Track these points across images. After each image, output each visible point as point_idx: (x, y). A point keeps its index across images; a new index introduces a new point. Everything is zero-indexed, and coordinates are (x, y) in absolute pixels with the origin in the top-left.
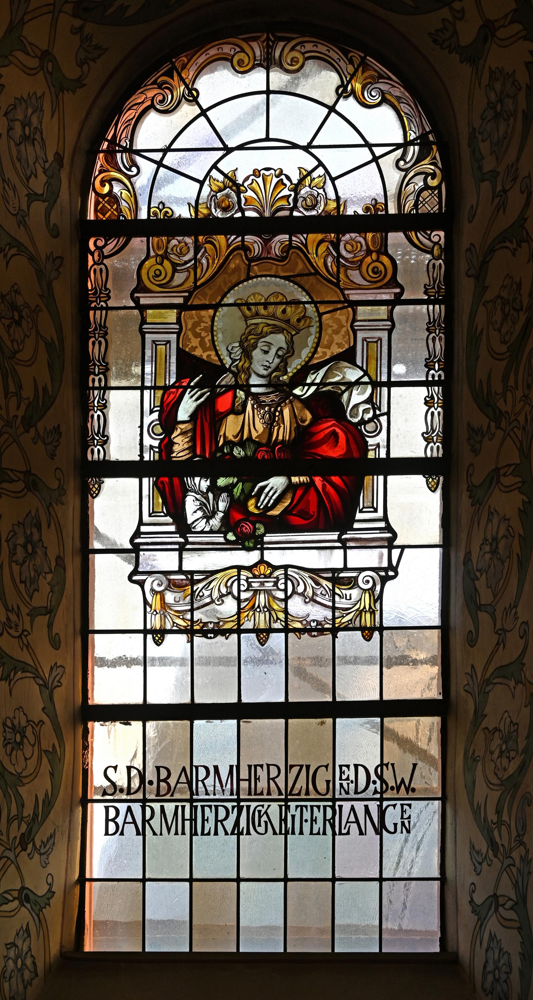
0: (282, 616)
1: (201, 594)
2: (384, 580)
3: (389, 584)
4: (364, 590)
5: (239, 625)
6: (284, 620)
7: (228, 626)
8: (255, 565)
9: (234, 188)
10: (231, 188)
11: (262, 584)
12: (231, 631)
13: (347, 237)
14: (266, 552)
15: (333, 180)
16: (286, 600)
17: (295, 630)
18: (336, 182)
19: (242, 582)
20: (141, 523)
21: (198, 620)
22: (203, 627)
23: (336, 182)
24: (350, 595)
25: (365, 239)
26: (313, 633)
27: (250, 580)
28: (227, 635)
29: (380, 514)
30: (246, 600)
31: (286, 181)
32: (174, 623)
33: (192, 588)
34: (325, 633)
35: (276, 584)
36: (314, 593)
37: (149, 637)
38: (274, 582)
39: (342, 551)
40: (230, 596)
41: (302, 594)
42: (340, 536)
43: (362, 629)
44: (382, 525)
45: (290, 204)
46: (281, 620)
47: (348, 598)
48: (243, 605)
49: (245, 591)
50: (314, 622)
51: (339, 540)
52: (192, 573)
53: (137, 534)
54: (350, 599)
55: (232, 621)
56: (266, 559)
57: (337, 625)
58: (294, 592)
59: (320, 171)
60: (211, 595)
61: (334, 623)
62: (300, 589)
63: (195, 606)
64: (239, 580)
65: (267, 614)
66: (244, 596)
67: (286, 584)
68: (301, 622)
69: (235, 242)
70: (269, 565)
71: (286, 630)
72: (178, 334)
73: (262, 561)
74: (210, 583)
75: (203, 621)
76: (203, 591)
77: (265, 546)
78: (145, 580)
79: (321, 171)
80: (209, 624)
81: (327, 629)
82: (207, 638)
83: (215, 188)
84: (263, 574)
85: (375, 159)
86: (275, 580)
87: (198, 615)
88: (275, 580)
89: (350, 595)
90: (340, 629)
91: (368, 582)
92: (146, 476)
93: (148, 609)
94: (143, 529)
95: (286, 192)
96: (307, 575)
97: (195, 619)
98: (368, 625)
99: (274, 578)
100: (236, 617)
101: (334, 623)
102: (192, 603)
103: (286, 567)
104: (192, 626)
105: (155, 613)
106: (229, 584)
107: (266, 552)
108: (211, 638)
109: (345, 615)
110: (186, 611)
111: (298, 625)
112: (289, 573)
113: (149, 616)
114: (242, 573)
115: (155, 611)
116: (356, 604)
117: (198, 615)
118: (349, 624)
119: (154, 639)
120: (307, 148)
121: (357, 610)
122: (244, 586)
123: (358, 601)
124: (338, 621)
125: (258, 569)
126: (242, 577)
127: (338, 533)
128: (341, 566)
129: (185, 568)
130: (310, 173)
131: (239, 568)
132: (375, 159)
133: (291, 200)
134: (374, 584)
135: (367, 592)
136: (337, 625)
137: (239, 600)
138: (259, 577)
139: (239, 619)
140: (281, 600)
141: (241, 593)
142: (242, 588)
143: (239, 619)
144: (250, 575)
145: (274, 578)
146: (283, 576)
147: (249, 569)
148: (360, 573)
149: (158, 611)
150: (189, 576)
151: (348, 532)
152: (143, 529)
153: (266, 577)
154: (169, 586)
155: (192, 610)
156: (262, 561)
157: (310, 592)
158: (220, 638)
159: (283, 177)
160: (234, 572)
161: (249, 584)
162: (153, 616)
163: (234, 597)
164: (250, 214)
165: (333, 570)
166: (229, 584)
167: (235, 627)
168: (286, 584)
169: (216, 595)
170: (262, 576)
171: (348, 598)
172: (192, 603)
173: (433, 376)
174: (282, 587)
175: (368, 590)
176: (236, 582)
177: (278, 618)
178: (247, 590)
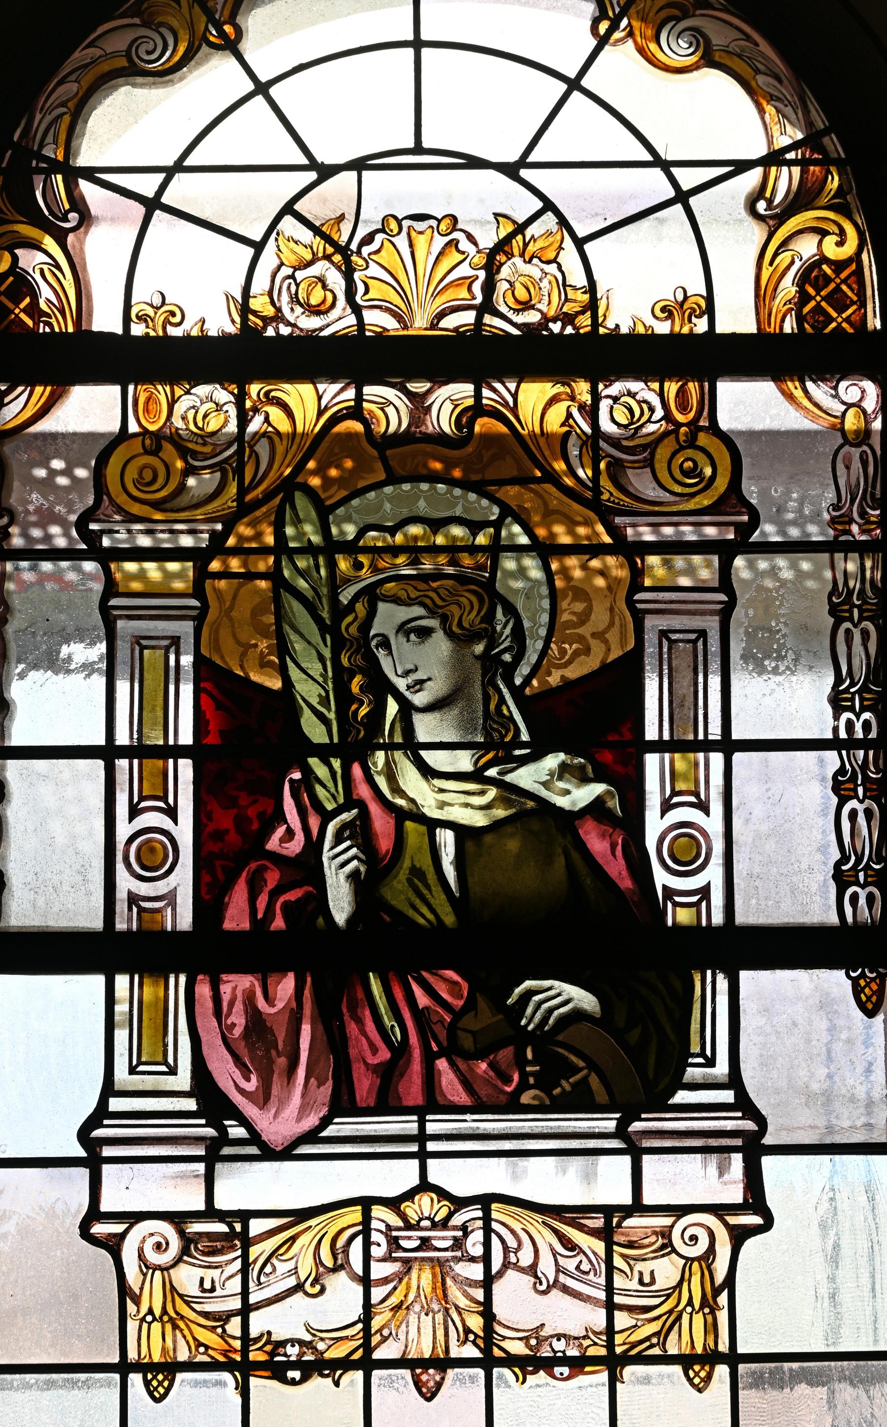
0: (476, 1323)
1: (268, 1269)
2: (739, 1236)
3: (751, 1245)
4: (689, 1260)
5: (367, 1347)
6: (481, 1334)
7: (338, 1352)
8: (409, 1195)
9: (337, 258)
10: (327, 257)
11: (425, 1244)
12: (345, 1364)
13: (616, 388)
14: (431, 1163)
15: (580, 243)
16: (488, 1282)
17: (510, 1361)
18: (588, 247)
19: (375, 1237)
20: (109, 1089)
21: (262, 1335)
22: (273, 1354)
23: (588, 247)
24: (652, 1272)
25: (661, 394)
26: (557, 1370)
27: (394, 1233)
28: (338, 1373)
29: (722, 1068)
30: (385, 1281)
31: (465, 245)
32: (199, 1344)
33: (245, 1256)
34: (587, 1369)
35: (458, 1244)
36: (559, 1270)
37: (136, 1380)
38: (455, 1239)
39: (627, 1160)
40: (342, 1275)
41: (532, 1270)
42: (622, 1125)
43: (686, 1361)
44: (727, 1096)
45: (474, 298)
46: (476, 1336)
47: (647, 1279)
48: (377, 1294)
49: (383, 1260)
50: (559, 1340)
51: (621, 1132)
52: (245, 1216)
53: (100, 1114)
54: (653, 1281)
55: (352, 1338)
56: (432, 1179)
57: (618, 1350)
58: (506, 1265)
59: (549, 220)
60: (295, 1271)
61: (610, 1345)
62: (526, 1258)
63: (253, 1299)
64: (366, 1231)
65: (439, 1317)
66: (379, 1270)
67: (487, 1244)
68: (526, 1339)
69: (335, 401)
70: (442, 1194)
71: (487, 1363)
72: (199, 619)
73: (424, 1186)
74: (293, 1239)
75: (274, 1338)
76: (274, 1260)
77: (431, 1146)
78: (123, 1236)
79: (549, 220)
80: (289, 1346)
81: (596, 1361)
82: (284, 1380)
83: (288, 257)
84: (428, 1218)
85: (682, 197)
86: (460, 1234)
87: (258, 1323)
88: (460, 1234)
89: (652, 1272)
90: (627, 1359)
91: (694, 1238)
92: (122, 971)
93: (131, 1308)
94: (116, 1104)
95: (464, 270)
96: (540, 1220)
97: (254, 1333)
98: (699, 1350)
99: (455, 1228)
100: (360, 1326)
101: (610, 1345)
102: (245, 1293)
103: (485, 1201)
104: (245, 1351)
105: (149, 1318)
106: (341, 1242)
107: (431, 1163)
108: (293, 1382)
109: (639, 1324)
110: (230, 1315)
111: (517, 1348)
112: (494, 1215)
113: (132, 1326)
114: (374, 1214)
115: (150, 1311)
116: (668, 1296)
117: (258, 1323)
118: (652, 1346)
119: (147, 1383)
120: (511, 170)
121: (670, 1312)
122: (379, 1245)
123: (674, 1288)
124: (618, 1339)
125: (416, 1207)
126: (375, 1224)
127: (618, 1116)
128: (626, 1199)
129: (222, 1203)
130: (520, 228)
131: (366, 1203)
132: (682, 197)
133: (477, 288)
134: (711, 1250)
135: (696, 1265)
136: (618, 1350)
137: (366, 1281)
138: (417, 1227)
139: (367, 1333)
140: (473, 1284)
141: (373, 1264)
142: (377, 1252)
143: (367, 1333)
144: (395, 1220)
145: (455, 1228)
146: (480, 1223)
147: (393, 1204)
148: (679, 1217)
149: (157, 1315)
150: (238, 1227)
151: (643, 1116)
152: (116, 1104)
153: (434, 1226)
154: (185, 1251)
155: (246, 1311)
156: (424, 1186)
157: (547, 1267)
158: (319, 1384)
159: (456, 235)
160: (354, 1215)
161: (394, 1243)
162: (145, 1326)
163: (354, 1277)
164: (377, 320)
165: (608, 1211)
166: (341, 1242)
167: (357, 1356)
168: (487, 1244)
169: (306, 1267)
170: (426, 1223)
171: (647, 1279)
172: (245, 1293)
173: (850, 725)
174: (477, 1251)
175: (698, 1259)
176: (360, 1239)
177: (468, 1331)
178: (387, 1258)
